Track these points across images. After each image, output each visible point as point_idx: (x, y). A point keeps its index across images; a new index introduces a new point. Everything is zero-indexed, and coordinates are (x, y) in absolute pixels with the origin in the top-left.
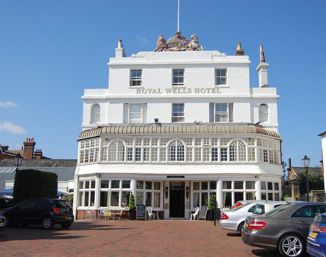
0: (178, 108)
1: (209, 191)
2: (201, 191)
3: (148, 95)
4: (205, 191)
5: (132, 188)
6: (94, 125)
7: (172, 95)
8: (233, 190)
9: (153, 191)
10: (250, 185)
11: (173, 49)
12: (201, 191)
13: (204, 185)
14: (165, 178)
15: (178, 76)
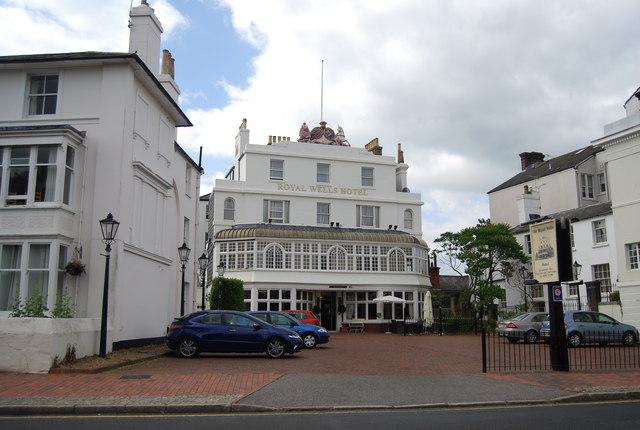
0: (323, 209)
1: (367, 302)
2: (357, 302)
3: (290, 192)
4: (361, 302)
5: (293, 301)
6: (230, 223)
7: (316, 194)
8: (268, 300)
9: (307, 302)
10: (409, 295)
11: (320, 140)
12: (357, 302)
13: (361, 295)
14: (327, 288)
15: (323, 171)
